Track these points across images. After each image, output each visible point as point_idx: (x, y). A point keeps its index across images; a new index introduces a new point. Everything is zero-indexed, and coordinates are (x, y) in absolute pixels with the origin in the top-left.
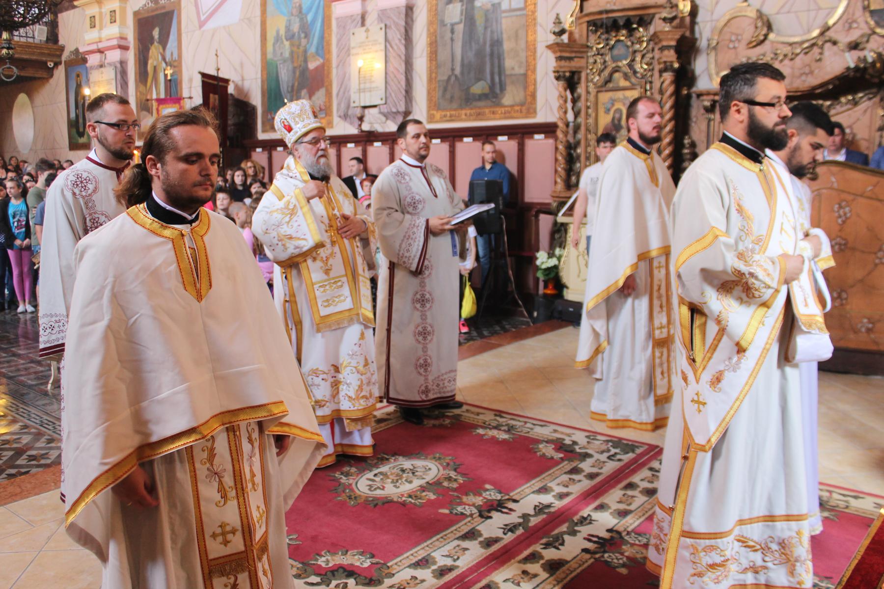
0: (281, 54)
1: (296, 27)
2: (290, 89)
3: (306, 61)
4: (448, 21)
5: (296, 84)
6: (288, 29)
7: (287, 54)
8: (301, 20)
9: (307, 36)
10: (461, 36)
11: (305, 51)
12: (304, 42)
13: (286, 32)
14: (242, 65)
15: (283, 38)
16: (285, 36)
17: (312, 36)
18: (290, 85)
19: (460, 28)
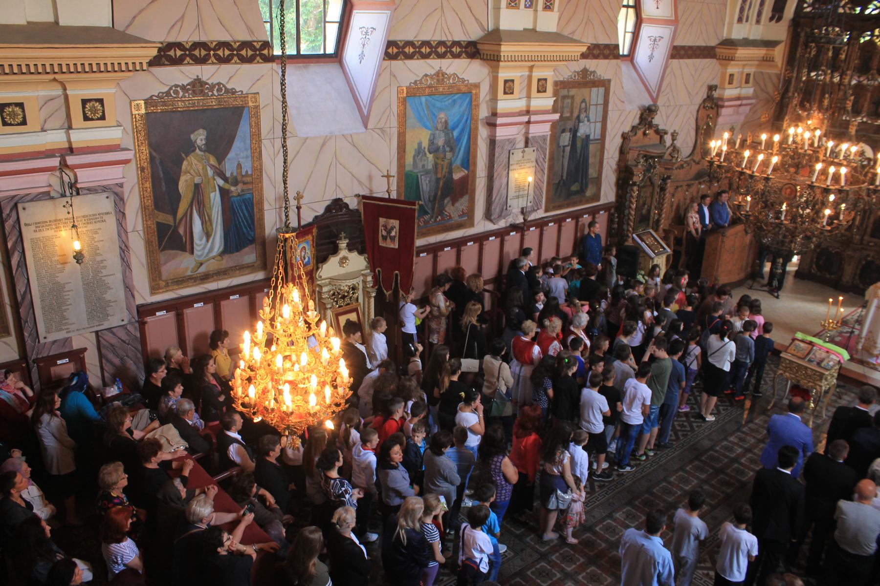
0: (423, 166)
1: (440, 142)
2: (431, 199)
3: (450, 172)
4: (561, 144)
5: (439, 193)
6: (432, 142)
7: (430, 166)
8: (447, 134)
9: (452, 150)
10: (568, 154)
11: (450, 164)
12: (449, 155)
13: (429, 146)
14: (370, 178)
15: (426, 150)
16: (428, 149)
17: (457, 150)
18: (433, 194)
19: (568, 149)
